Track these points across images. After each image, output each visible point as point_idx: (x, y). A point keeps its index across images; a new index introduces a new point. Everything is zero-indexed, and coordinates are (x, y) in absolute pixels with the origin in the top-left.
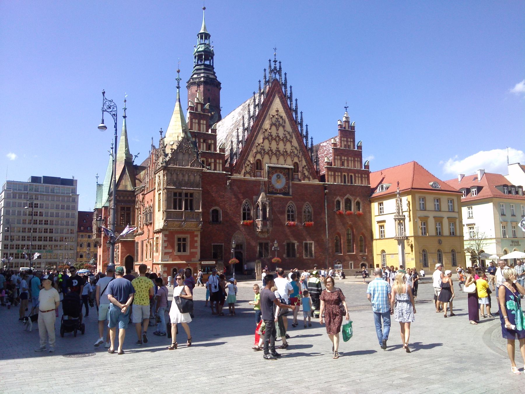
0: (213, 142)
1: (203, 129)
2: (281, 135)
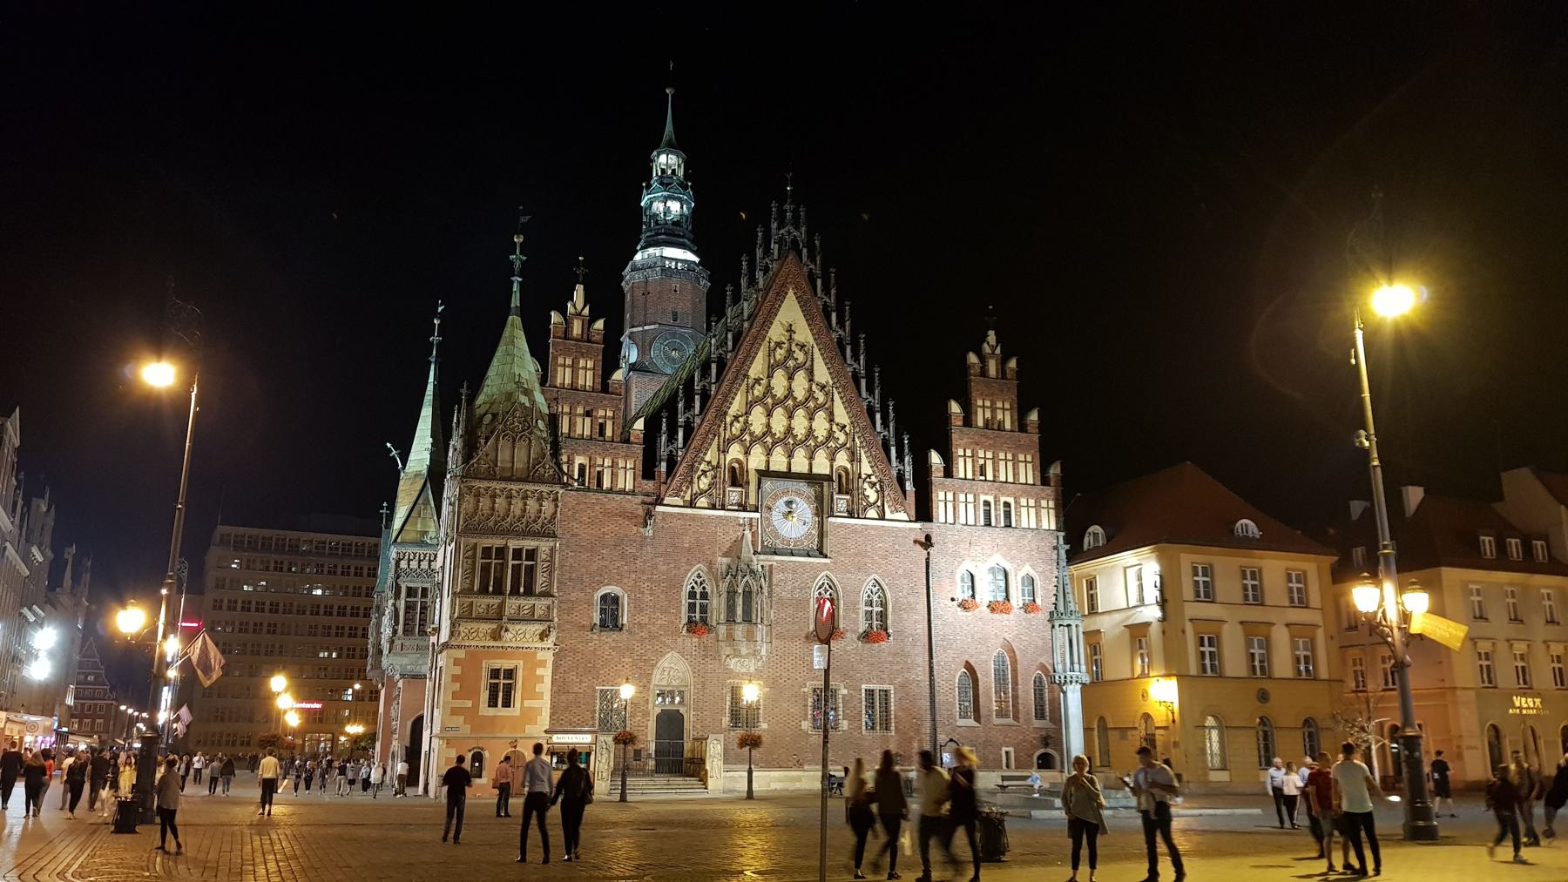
0: (610, 414)
2: (800, 394)
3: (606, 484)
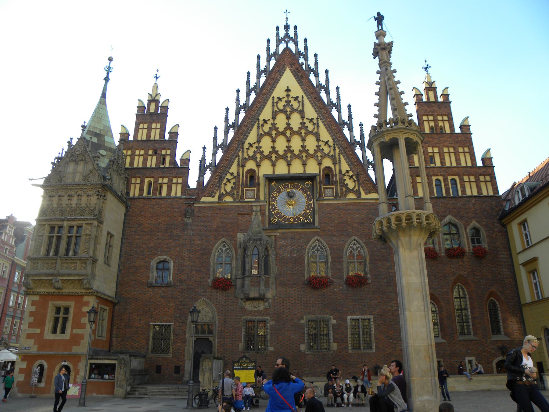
0: (169, 152)
1: (155, 135)
3: (164, 194)
